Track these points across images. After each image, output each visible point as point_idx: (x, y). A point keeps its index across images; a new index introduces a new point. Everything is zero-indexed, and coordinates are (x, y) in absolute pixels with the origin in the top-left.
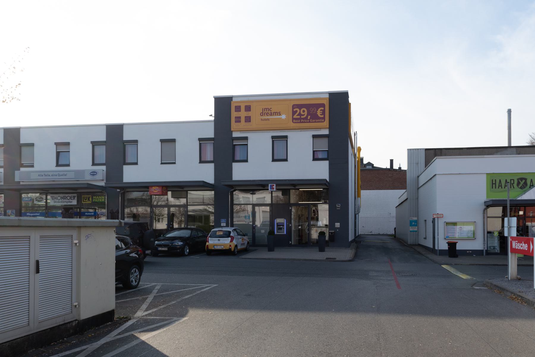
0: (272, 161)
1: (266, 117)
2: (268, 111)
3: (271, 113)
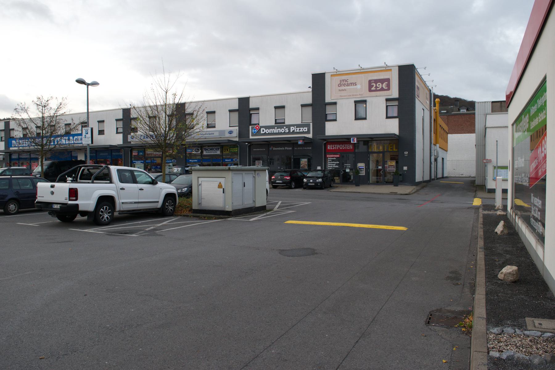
0: (355, 120)
1: (343, 88)
2: (345, 82)
3: (348, 83)
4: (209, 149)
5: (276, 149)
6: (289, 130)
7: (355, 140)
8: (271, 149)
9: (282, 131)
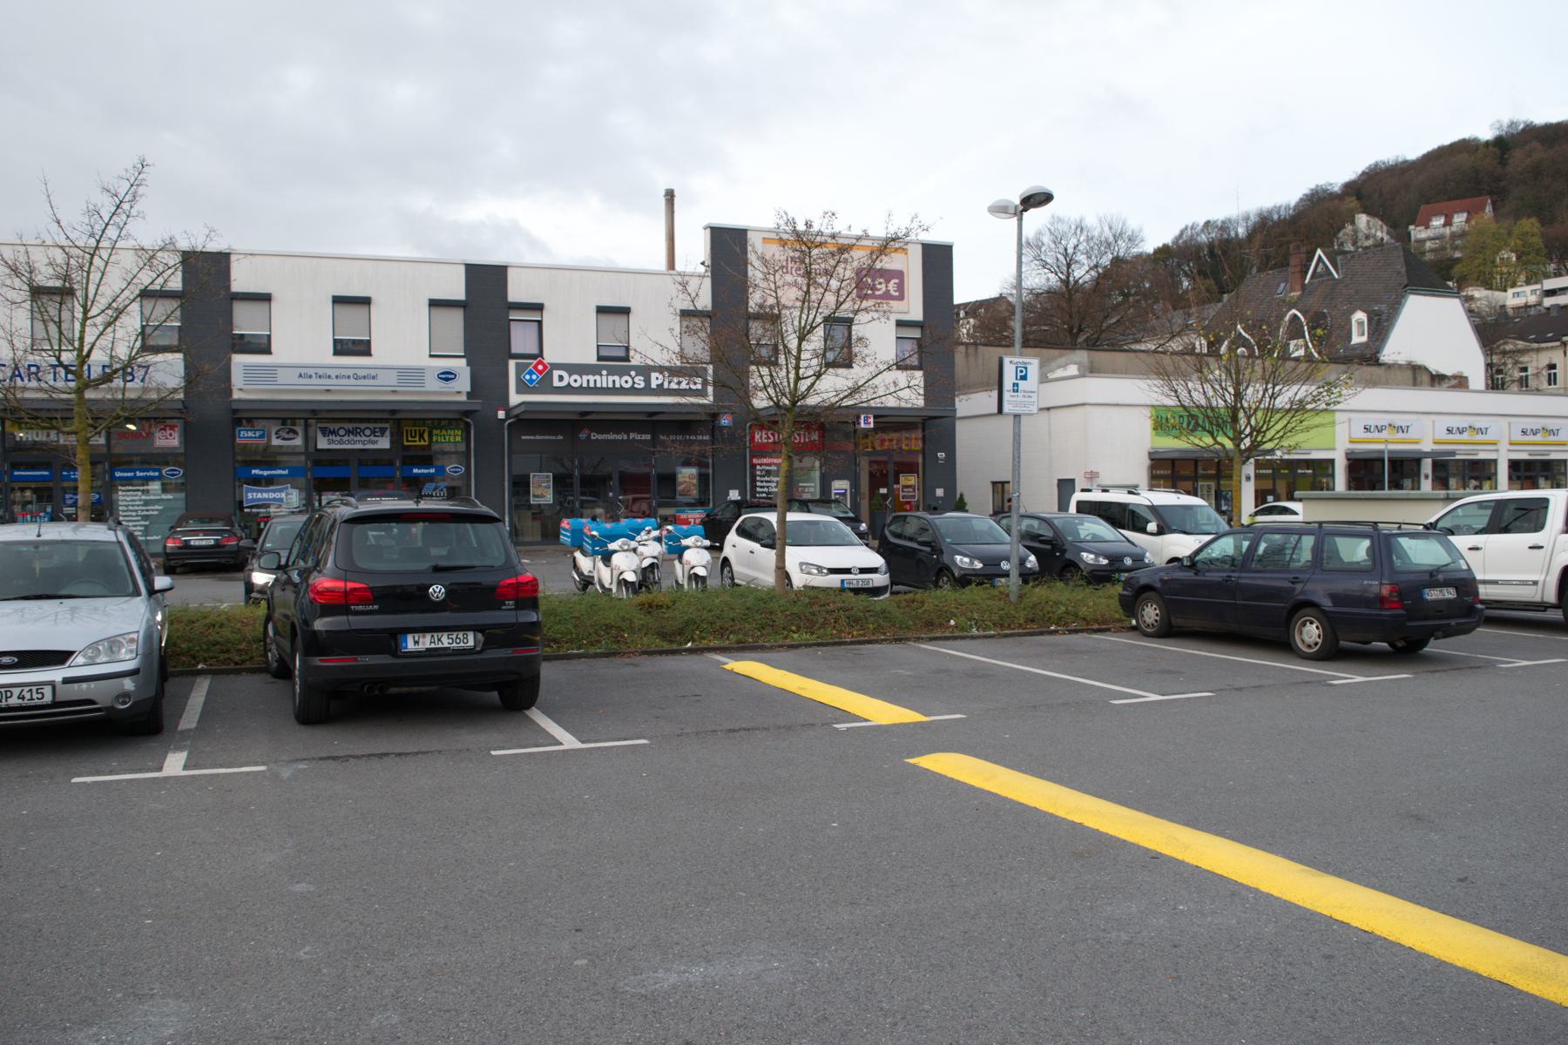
4: (342, 432)
5: (600, 437)
6: (648, 381)
8: (583, 436)
9: (624, 381)
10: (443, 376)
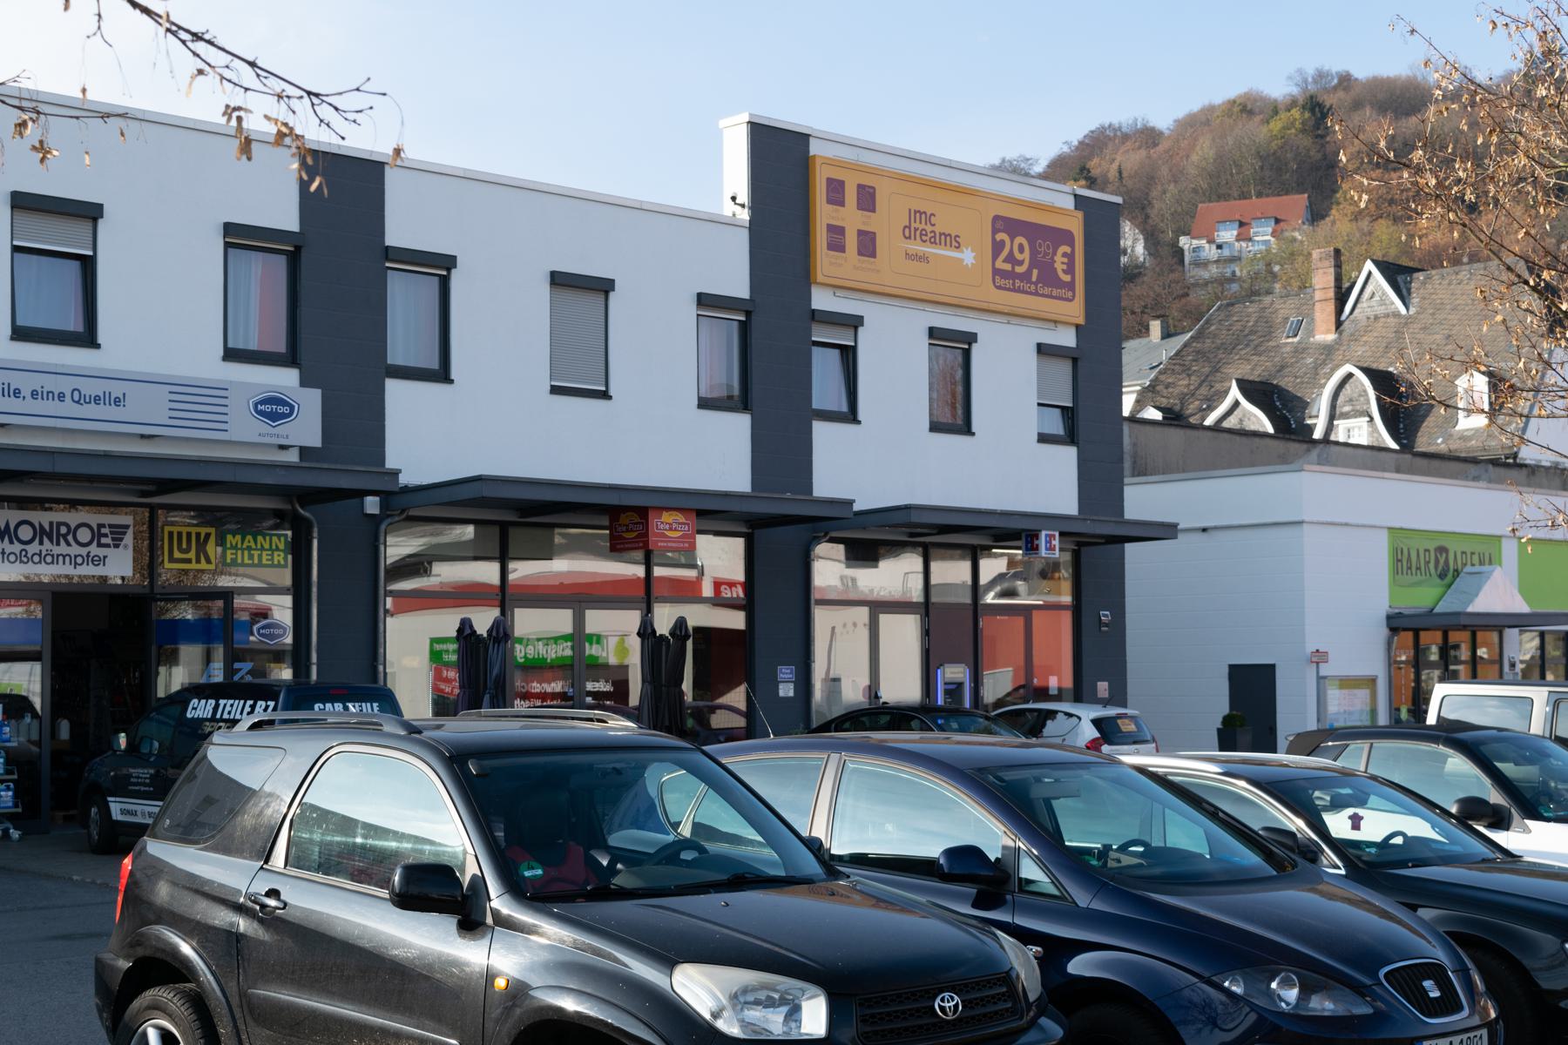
2: (926, 224)
4: (25, 533)
7: (1053, 542)
10: (267, 408)
